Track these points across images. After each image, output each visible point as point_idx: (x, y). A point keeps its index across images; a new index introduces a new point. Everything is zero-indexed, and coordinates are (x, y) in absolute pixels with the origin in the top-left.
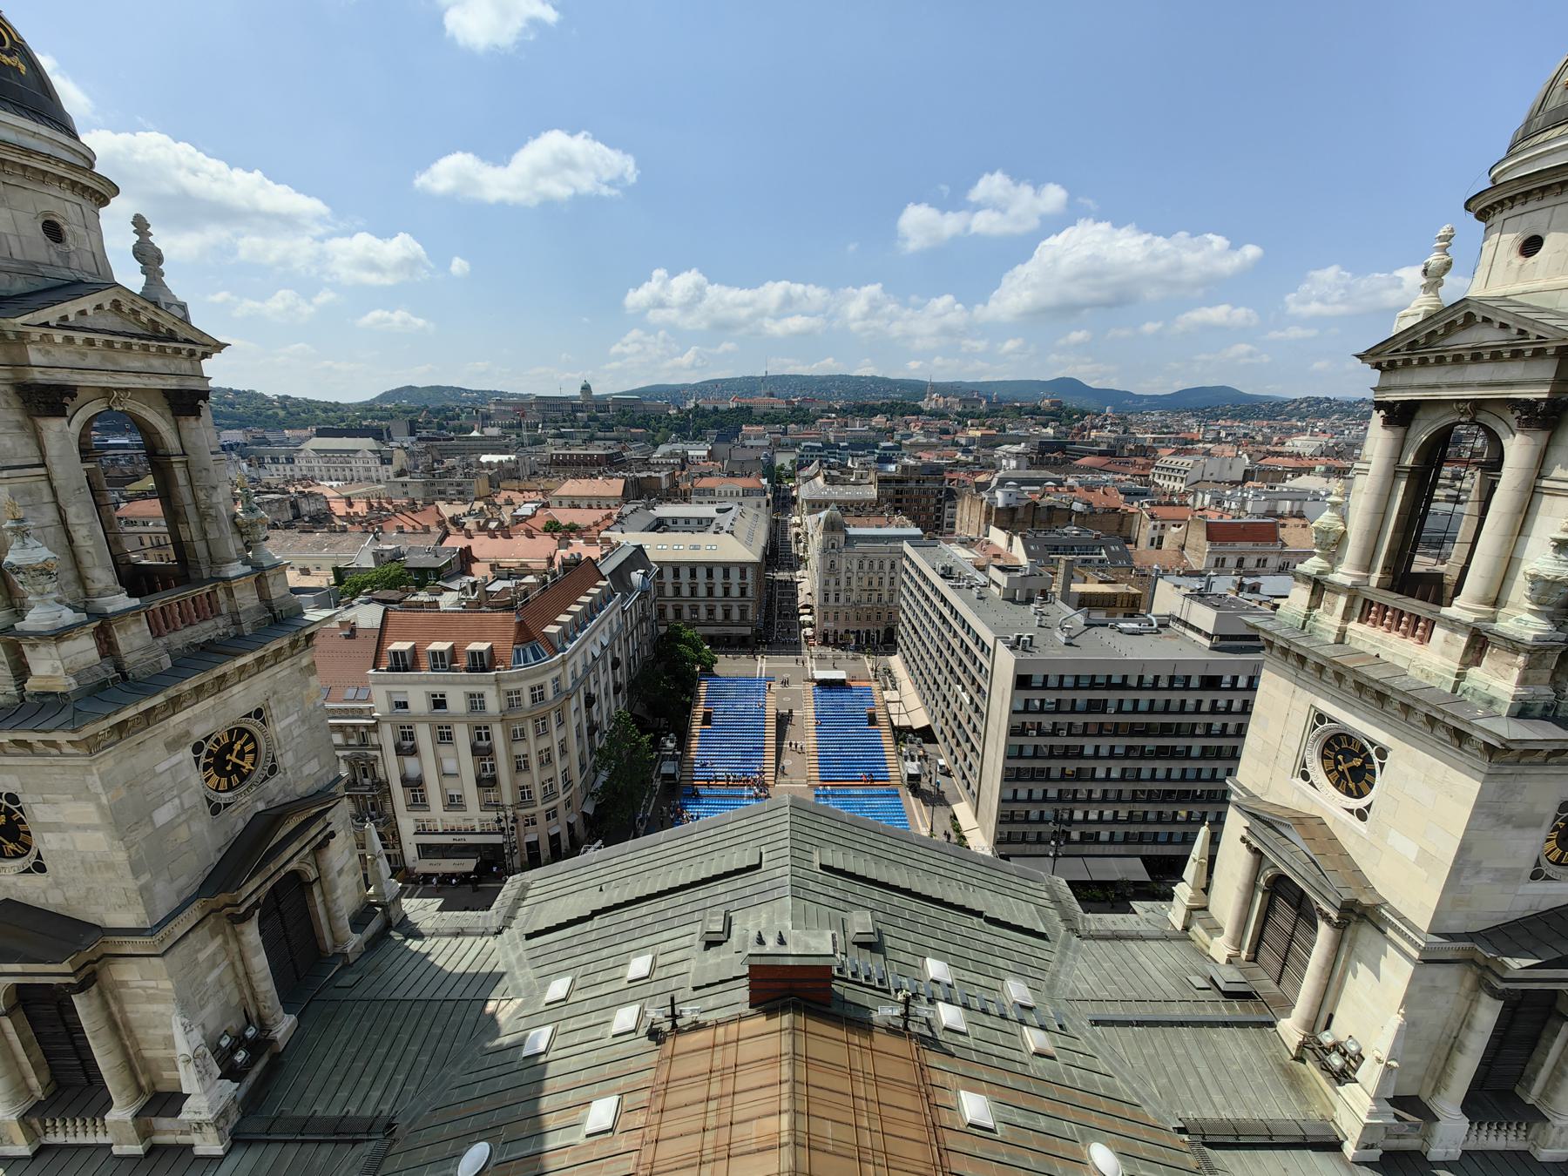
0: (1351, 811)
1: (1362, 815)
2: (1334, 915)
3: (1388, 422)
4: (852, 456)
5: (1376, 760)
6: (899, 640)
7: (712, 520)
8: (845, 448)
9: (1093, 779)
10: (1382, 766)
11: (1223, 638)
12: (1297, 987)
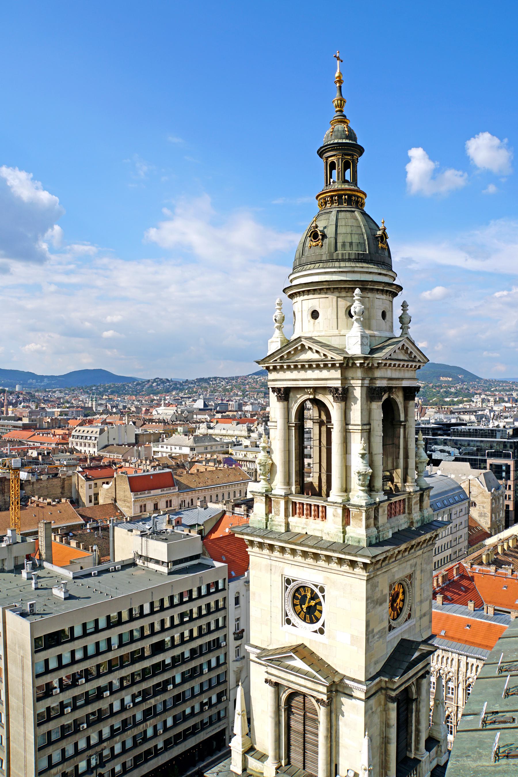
0: (316, 632)
1: (321, 631)
2: (325, 698)
3: (280, 399)
5: (320, 595)
9: (113, 714)
10: (324, 596)
11: (175, 563)
12: (315, 762)
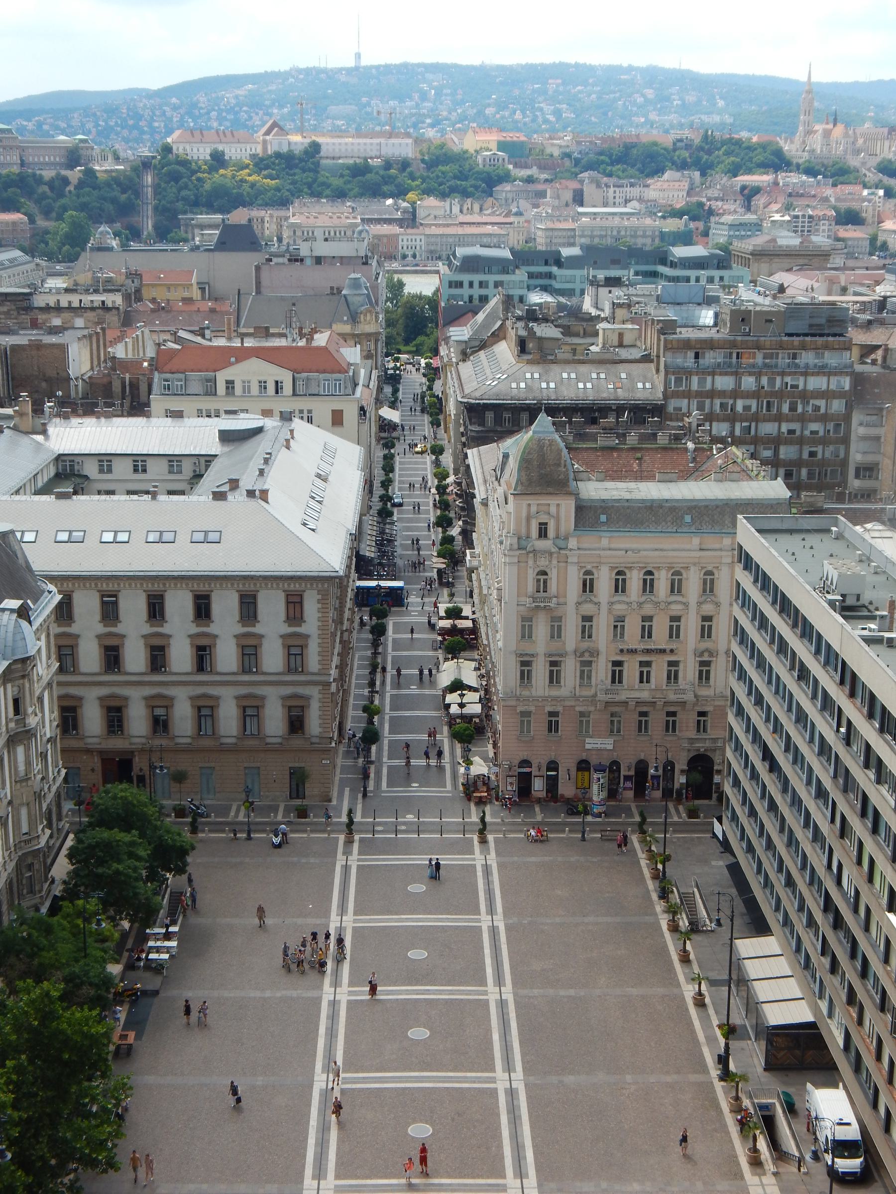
4: (594, 283)
6: (728, 789)
7: (209, 459)
8: (575, 262)
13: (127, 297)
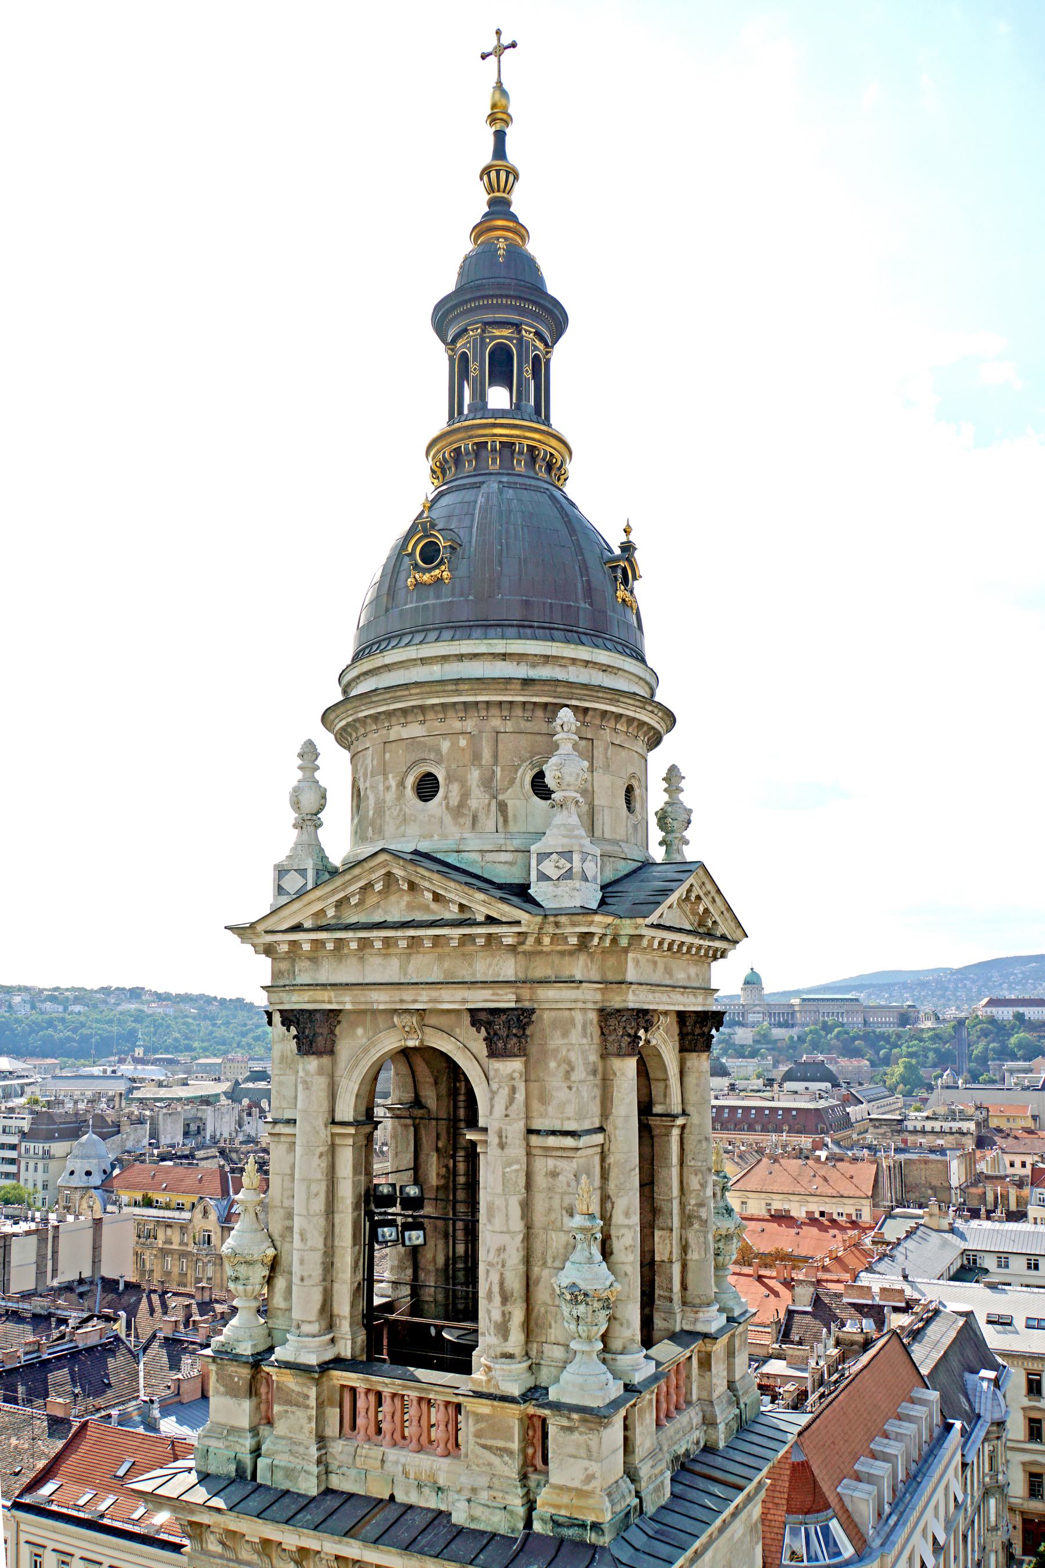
13: (978, 1124)
